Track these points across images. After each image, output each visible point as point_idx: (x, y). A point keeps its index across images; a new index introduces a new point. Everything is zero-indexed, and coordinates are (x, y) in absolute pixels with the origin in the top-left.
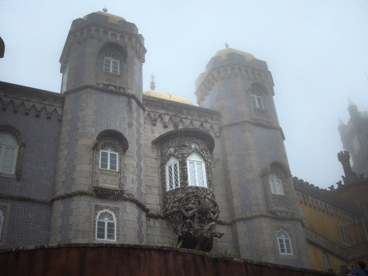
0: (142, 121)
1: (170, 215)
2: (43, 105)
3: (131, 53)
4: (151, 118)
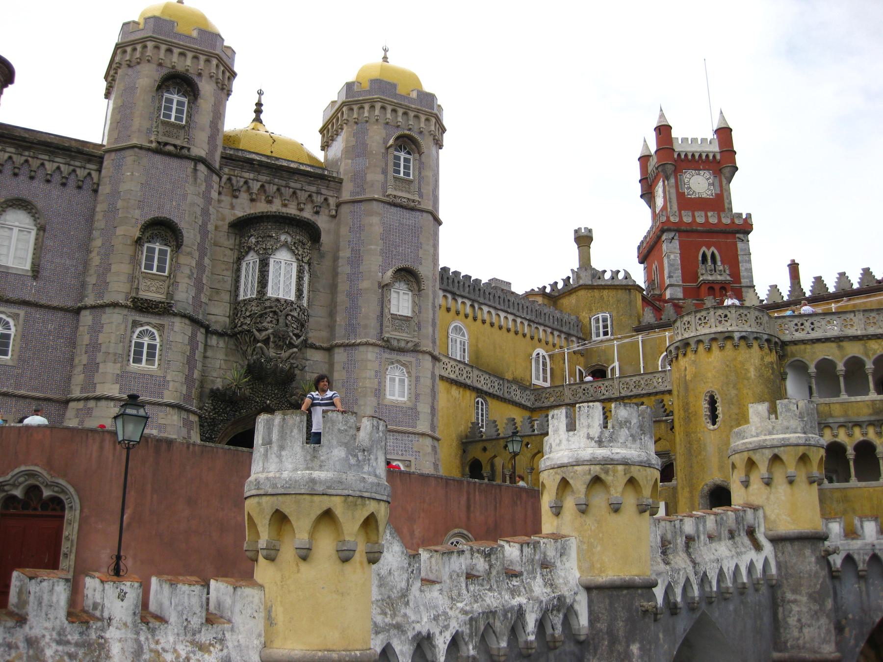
0: (214, 195)
1: (239, 333)
2: (72, 168)
3: (206, 88)
4: (232, 185)
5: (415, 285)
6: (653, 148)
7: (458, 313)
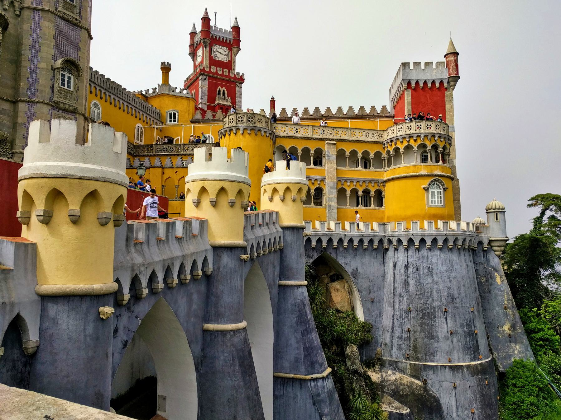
5: (76, 73)
6: (199, 28)
7: (96, 96)
